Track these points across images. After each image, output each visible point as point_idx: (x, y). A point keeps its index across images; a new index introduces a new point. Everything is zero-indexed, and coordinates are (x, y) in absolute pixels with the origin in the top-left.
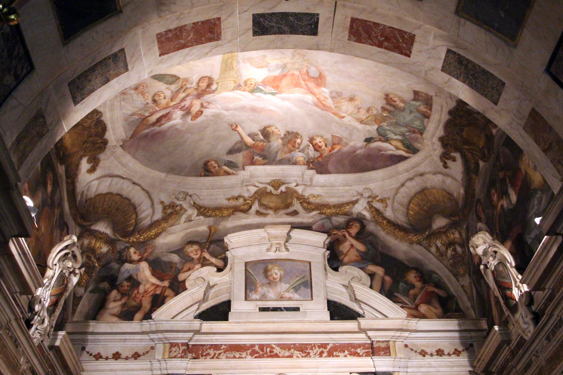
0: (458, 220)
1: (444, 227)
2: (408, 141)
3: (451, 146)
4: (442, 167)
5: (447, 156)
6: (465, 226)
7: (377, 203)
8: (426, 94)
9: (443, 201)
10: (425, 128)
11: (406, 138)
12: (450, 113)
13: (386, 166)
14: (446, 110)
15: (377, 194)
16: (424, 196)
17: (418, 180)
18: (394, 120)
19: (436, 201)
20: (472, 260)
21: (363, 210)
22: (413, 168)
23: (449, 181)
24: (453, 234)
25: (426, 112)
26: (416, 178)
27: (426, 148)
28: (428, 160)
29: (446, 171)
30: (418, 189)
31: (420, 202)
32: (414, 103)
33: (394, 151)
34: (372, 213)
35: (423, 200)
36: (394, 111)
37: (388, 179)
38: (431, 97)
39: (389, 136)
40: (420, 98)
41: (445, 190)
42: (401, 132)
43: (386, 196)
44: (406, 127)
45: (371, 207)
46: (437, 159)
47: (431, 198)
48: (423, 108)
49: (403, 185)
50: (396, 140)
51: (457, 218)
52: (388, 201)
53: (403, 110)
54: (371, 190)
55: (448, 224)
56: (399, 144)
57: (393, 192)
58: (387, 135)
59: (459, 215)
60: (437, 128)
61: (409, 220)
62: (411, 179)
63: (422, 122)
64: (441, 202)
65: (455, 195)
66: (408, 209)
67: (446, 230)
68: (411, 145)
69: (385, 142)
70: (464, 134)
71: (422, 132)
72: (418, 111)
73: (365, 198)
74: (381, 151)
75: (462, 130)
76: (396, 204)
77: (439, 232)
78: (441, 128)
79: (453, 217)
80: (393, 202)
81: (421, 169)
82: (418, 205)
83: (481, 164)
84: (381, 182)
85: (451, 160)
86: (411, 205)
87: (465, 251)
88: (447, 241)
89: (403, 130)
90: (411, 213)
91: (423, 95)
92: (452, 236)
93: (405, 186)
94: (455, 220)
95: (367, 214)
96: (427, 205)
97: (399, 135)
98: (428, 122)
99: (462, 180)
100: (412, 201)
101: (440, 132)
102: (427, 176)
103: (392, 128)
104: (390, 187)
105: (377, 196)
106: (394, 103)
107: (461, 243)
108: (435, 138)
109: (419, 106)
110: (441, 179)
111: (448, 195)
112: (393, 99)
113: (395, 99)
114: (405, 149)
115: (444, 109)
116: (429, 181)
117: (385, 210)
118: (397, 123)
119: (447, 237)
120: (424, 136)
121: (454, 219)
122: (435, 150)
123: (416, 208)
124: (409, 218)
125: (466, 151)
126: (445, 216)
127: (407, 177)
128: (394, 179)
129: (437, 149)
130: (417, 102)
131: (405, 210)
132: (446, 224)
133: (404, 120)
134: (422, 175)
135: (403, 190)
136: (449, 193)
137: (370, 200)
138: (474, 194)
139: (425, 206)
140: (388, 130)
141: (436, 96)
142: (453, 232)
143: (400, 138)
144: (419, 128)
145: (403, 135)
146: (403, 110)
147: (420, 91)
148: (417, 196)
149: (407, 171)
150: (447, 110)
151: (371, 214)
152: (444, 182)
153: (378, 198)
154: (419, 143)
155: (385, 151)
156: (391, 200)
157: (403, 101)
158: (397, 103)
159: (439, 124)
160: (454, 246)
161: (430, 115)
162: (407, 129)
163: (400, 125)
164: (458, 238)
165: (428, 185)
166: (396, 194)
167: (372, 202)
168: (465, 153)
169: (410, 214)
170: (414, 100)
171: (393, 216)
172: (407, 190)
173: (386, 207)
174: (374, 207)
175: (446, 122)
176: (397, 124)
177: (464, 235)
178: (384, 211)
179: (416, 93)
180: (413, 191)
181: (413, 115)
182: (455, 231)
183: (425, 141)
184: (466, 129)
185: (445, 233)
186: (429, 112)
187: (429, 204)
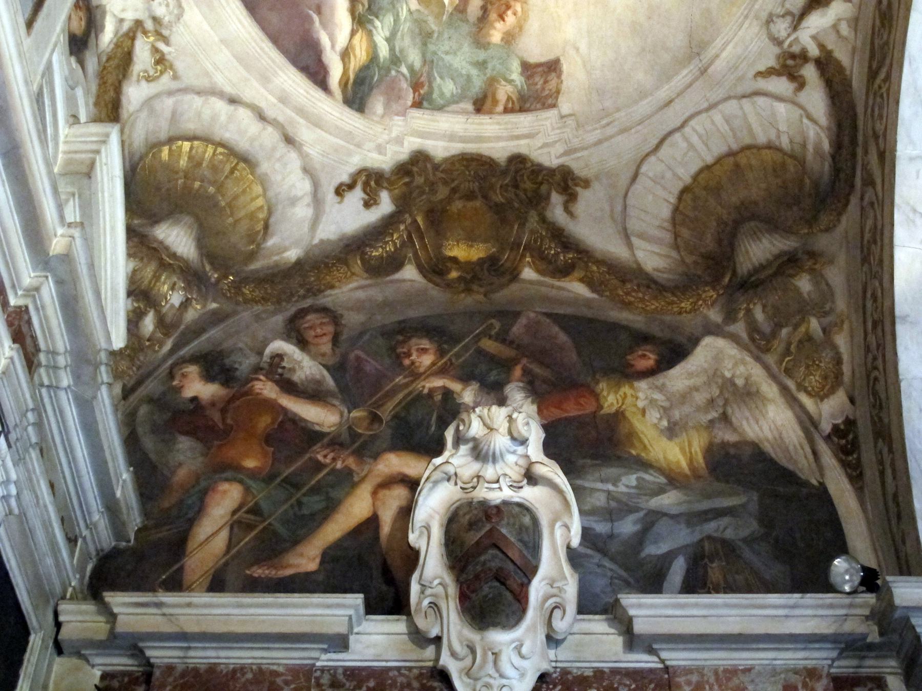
0: (213, 280)
1: (174, 255)
2: (380, 80)
3: (406, 184)
4: (335, 183)
5: (372, 183)
6: (214, 305)
7: (148, 47)
8: (558, 92)
9: (237, 222)
10: (440, 108)
11: (388, 70)
12: (518, 160)
13: (275, 39)
14: (522, 147)
15: (174, 39)
16: (228, 168)
17: (270, 136)
18: (434, 27)
19: (229, 205)
20: (171, 375)
21: (115, 16)
22: (301, 111)
23: (303, 211)
24: (173, 288)
25: (495, 102)
26: (270, 129)
27: (379, 128)
28: (342, 143)
29: (330, 196)
30: (242, 144)
31: (204, 165)
32: (516, 66)
33: (333, 47)
34: (117, 45)
35: (214, 168)
36: (467, 21)
37: (235, 56)
38: (554, 106)
39: (377, 23)
40: (539, 80)
41: (270, 213)
42: (401, 51)
43: (179, 65)
44: (424, 62)
45: (131, 36)
46: (355, 162)
47: (232, 189)
48: (503, 92)
49: (233, 101)
50: (373, 47)
51: (216, 276)
52: (166, 79)
53: (480, 42)
54: (179, 17)
55: (186, 261)
56: (360, 55)
57: (201, 82)
58: (377, 17)
59: (227, 277)
60: (452, 137)
61: (141, 158)
62: (261, 117)
63: (456, 99)
64: (232, 215)
65: (270, 243)
66: (171, 140)
67: (170, 264)
68: (371, 89)
69: (353, 19)
70: (458, 205)
71: (425, 104)
72: (492, 82)
73: (149, 9)
74: (319, 11)
75: (470, 196)
76: (169, 102)
77: (155, 249)
78: (457, 148)
79: (212, 264)
80: (170, 93)
81: (306, 134)
82: (195, 162)
83: (410, 273)
84: (216, 39)
85: (366, 197)
86: (186, 145)
87: (161, 344)
88: (146, 282)
89: (414, 57)
90: (165, 153)
91: (552, 84)
92: (166, 287)
93: (232, 108)
94: (205, 272)
95: (108, 36)
96: (206, 184)
97: (392, 50)
98: (464, 112)
99: (322, 242)
100: (196, 143)
101: (440, 149)
102: (293, 155)
103: (405, 26)
104: (210, 68)
105: (166, 40)
106: (493, 16)
107: (168, 319)
108: (419, 140)
109: (510, 82)
110: (300, 194)
111: (260, 226)
112: (509, 13)
113: (510, 18)
114: (352, 76)
115: (523, 142)
116: (278, 166)
117: (138, 81)
118: (429, 35)
119: (156, 277)
120: (415, 113)
121: (208, 268)
122: (380, 149)
123: (183, 162)
124: (147, 154)
125: (409, 221)
126: (201, 243)
127: (263, 105)
128: (241, 69)
129: (385, 155)
130: (522, 74)
131: (163, 136)
132: (185, 256)
133: (447, 53)
134: (289, 140)
135: (220, 105)
136: (266, 227)
137: (149, 25)
138: (320, 291)
139: (202, 181)
140: (397, 20)
141: (562, 117)
142: (174, 284)
143: (384, 51)
144: (435, 96)
145: (396, 59)
146: (480, 42)
147: (564, 77)
148: (220, 150)
149: (284, 99)
150: (524, 151)
151: (112, 46)
152: (293, 201)
153: (161, 46)
154: (387, 106)
155: (321, 23)
156: (174, 85)
157: (509, 38)
158: (499, 25)
159: (463, 140)
160: (146, 306)
161: (490, 112)
162: (417, 64)
163: (425, 44)
164: (172, 306)
165: (265, 167)
166: (199, 93)
167: (145, 33)
168: (404, 222)
169: (160, 151)
170: (527, 68)
171: (132, 109)
172: (223, 118)
173: (149, 79)
174: (133, 45)
175: (481, 156)
176: (425, 36)
177: (191, 315)
178: (134, 78)
179: (553, 67)
180: (229, 135)
181: (474, 72)
182: (184, 289)
183: (398, 120)
184: (478, 203)
185: (163, 266)
186: (500, 108)
187: (211, 190)
